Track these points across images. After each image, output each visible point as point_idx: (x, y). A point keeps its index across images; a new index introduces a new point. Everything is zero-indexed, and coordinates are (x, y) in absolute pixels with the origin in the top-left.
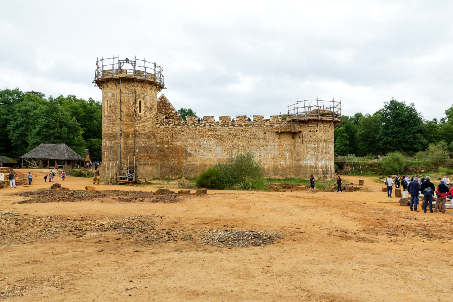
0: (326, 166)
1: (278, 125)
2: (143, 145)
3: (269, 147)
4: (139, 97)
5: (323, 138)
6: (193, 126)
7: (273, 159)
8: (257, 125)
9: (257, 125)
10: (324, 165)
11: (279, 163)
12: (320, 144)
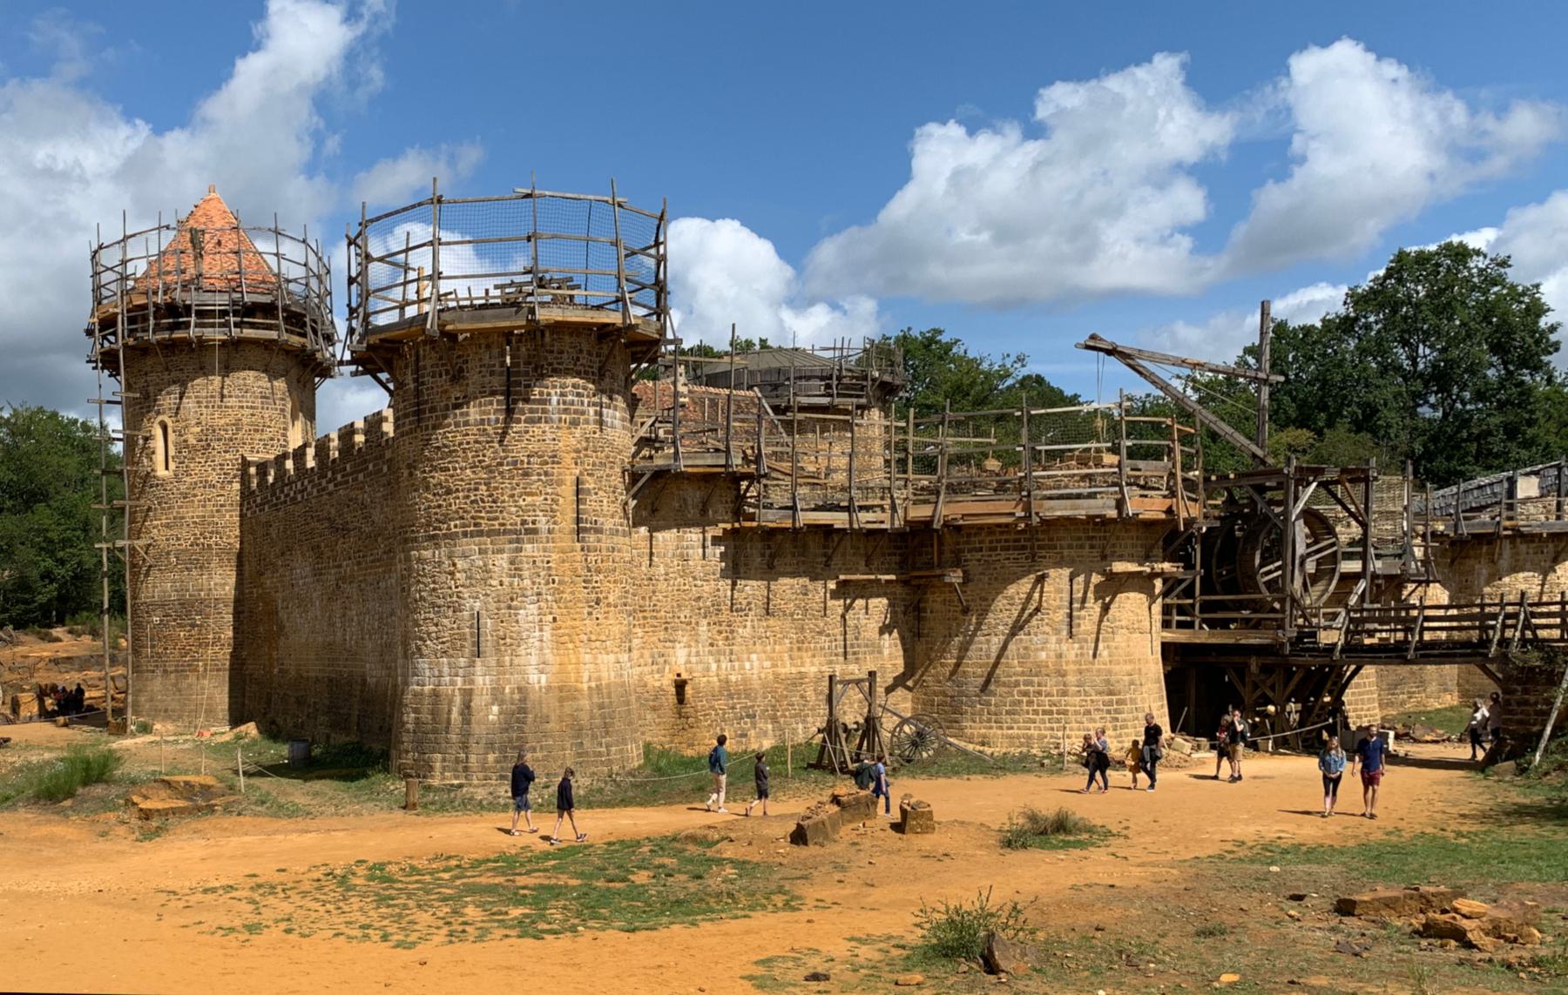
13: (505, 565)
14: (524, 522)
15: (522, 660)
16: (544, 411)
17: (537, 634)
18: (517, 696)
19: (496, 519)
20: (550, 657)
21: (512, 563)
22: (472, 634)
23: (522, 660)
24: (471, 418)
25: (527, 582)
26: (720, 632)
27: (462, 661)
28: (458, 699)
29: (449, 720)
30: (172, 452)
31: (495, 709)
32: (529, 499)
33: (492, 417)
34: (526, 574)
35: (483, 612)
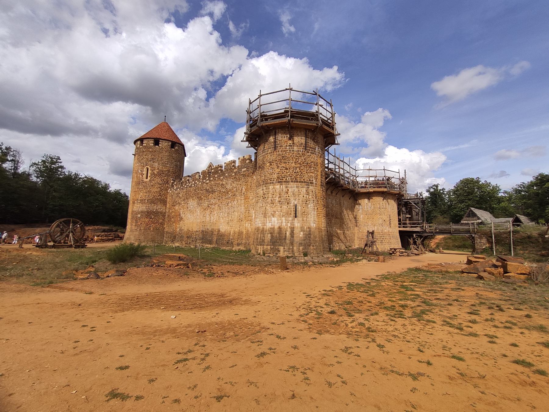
0: (280, 228)
1: (245, 169)
3: (235, 202)
5: (275, 176)
9: (227, 175)
10: (276, 227)
12: (271, 187)
13: (305, 191)
14: (310, 180)
24: (295, 149)
27: (290, 219)
28: (289, 230)
29: (286, 236)
30: (149, 175)
31: (302, 233)
34: (310, 194)
35: (297, 205)
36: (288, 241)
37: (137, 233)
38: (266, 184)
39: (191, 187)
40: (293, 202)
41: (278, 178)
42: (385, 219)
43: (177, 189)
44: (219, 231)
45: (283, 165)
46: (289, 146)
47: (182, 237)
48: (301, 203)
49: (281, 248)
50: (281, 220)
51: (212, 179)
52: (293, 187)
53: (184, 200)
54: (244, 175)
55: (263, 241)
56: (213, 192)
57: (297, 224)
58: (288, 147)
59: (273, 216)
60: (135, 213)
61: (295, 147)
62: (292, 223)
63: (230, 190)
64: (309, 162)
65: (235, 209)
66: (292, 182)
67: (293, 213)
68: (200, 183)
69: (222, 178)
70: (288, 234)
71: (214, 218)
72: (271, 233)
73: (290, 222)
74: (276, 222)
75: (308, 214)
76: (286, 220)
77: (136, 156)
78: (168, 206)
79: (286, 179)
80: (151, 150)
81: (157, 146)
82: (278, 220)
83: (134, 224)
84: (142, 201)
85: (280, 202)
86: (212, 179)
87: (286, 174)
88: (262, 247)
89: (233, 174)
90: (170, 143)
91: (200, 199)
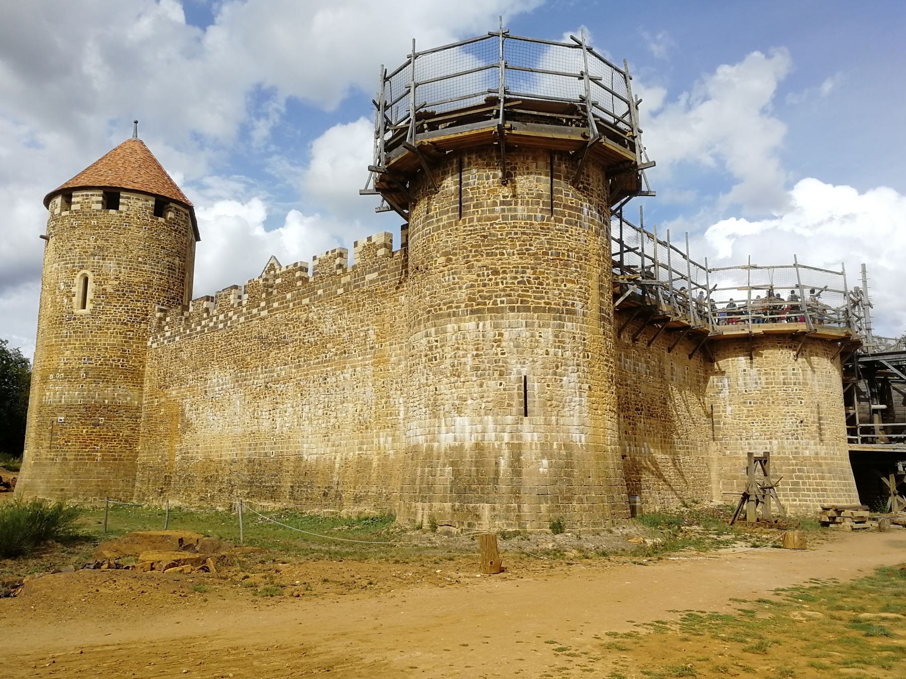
0: (478, 446)
1: (374, 275)
2: (80, 401)
4: (82, 268)
6: (199, 328)
7: (363, 426)
8: (320, 292)
9: (320, 292)
10: (468, 445)
11: (375, 440)
12: (449, 327)
13: (551, 338)
14: (565, 304)
15: (567, 420)
16: (579, 218)
17: (577, 399)
18: (563, 452)
19: (542, 298)
20: (587, 421)
21: (556, 336)
22: (519, 396)
23: (567, 420)
24: (519, 213)
25: (568, 354)
26: (629, 424)
27: (509, 419)
28: (506, 452)
29: (497, 473)
30: (90, 296)
31: (545, 462)
32: (569, 285)
33: (539, 215)
34: (568, 346)
36: (503, 487)
37: (55, 470)
38: (438, 317)
39: (215, 329)
40: (517, 369)
41: (470, 299)
42: (802, 415)
43: (171, 339)
44: (300, 459)
45: (486, 261)
46: (502, 203)
47: (189, 479)
48: (539, 371)
49: (485, 510)
50: (481, 422)
51: (276, 305)
52: (515, 327)
53: (195, 369)
54: (371, 294)
55: (431, 487)
56: (281, 343)
57: (530, 435)
58: (498, 208)
59: (460, 413)
60: (48, 411)
61: (520, 207)
62: (516, 433)
63: (332, 338)
64: (563, 249)
65: (348, 393)
66: (512, 309)
67: (517, 402)
68: (242, 319)
69: (306, 301)
70: (504, 464)
71: (285, 421)
72: (453, 464)
73: (508, 428)
74: (468, 429)
75: (561, 404)
76: (496, 422)
77: (52, 241)
78: (146, 389)
79: (495, 303)
80: (94, 222)
81: (112, 212)
82: (472, 423)
83: (46, 444)
84: (69, 375)
85: (477, 369)
86: (276, 305)
87: (493, 288)
88: (427, 505)
89: (340, 291)
90: (151, 203)
91: (242, 364)
